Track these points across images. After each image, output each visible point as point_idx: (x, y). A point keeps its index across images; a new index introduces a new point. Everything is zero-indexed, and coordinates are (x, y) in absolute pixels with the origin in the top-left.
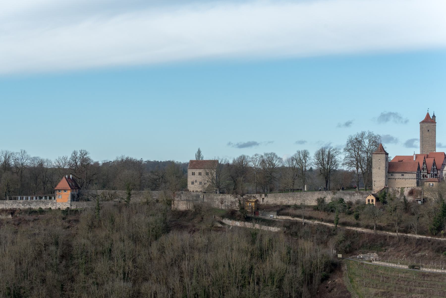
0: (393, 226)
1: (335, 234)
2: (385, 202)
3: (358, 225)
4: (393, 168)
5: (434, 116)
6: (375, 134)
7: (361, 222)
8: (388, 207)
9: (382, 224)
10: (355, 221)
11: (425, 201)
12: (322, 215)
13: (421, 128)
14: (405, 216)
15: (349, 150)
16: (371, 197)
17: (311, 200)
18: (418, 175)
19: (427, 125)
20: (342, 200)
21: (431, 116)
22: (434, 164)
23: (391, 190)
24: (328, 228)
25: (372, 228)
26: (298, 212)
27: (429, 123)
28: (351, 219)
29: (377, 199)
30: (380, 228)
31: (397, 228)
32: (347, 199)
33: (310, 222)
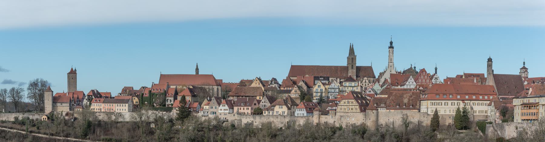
0: (59, 133)
1: (27, 137)
2: (53, 120)
3: (39, 133)
4: (56, 100)
5: (75, 70)
6: (45, 80)
7: (41, 131)
8: (55, 122)
9: (54, 133)
10: (37, 131)
11: (75, 119)
12: (19, 127)
13: (68, 77)
14: (65, 128)
15: (30, 89)
16: (45, 117)
17: (11, 117)
18: (70, 104)
19: (72, 75)
20: (28, 118)
21: (74, 70)
22: (78, 98)
23: (55, 112)
24: (23, 134)
25: (47, 134)
26: (4, 125)
27: (72, 75)
28: (34, 129)
29: (48, 118)
30: (52, 135)
31: (62, 135)
32: (31, 117)
33: (12, 130)
